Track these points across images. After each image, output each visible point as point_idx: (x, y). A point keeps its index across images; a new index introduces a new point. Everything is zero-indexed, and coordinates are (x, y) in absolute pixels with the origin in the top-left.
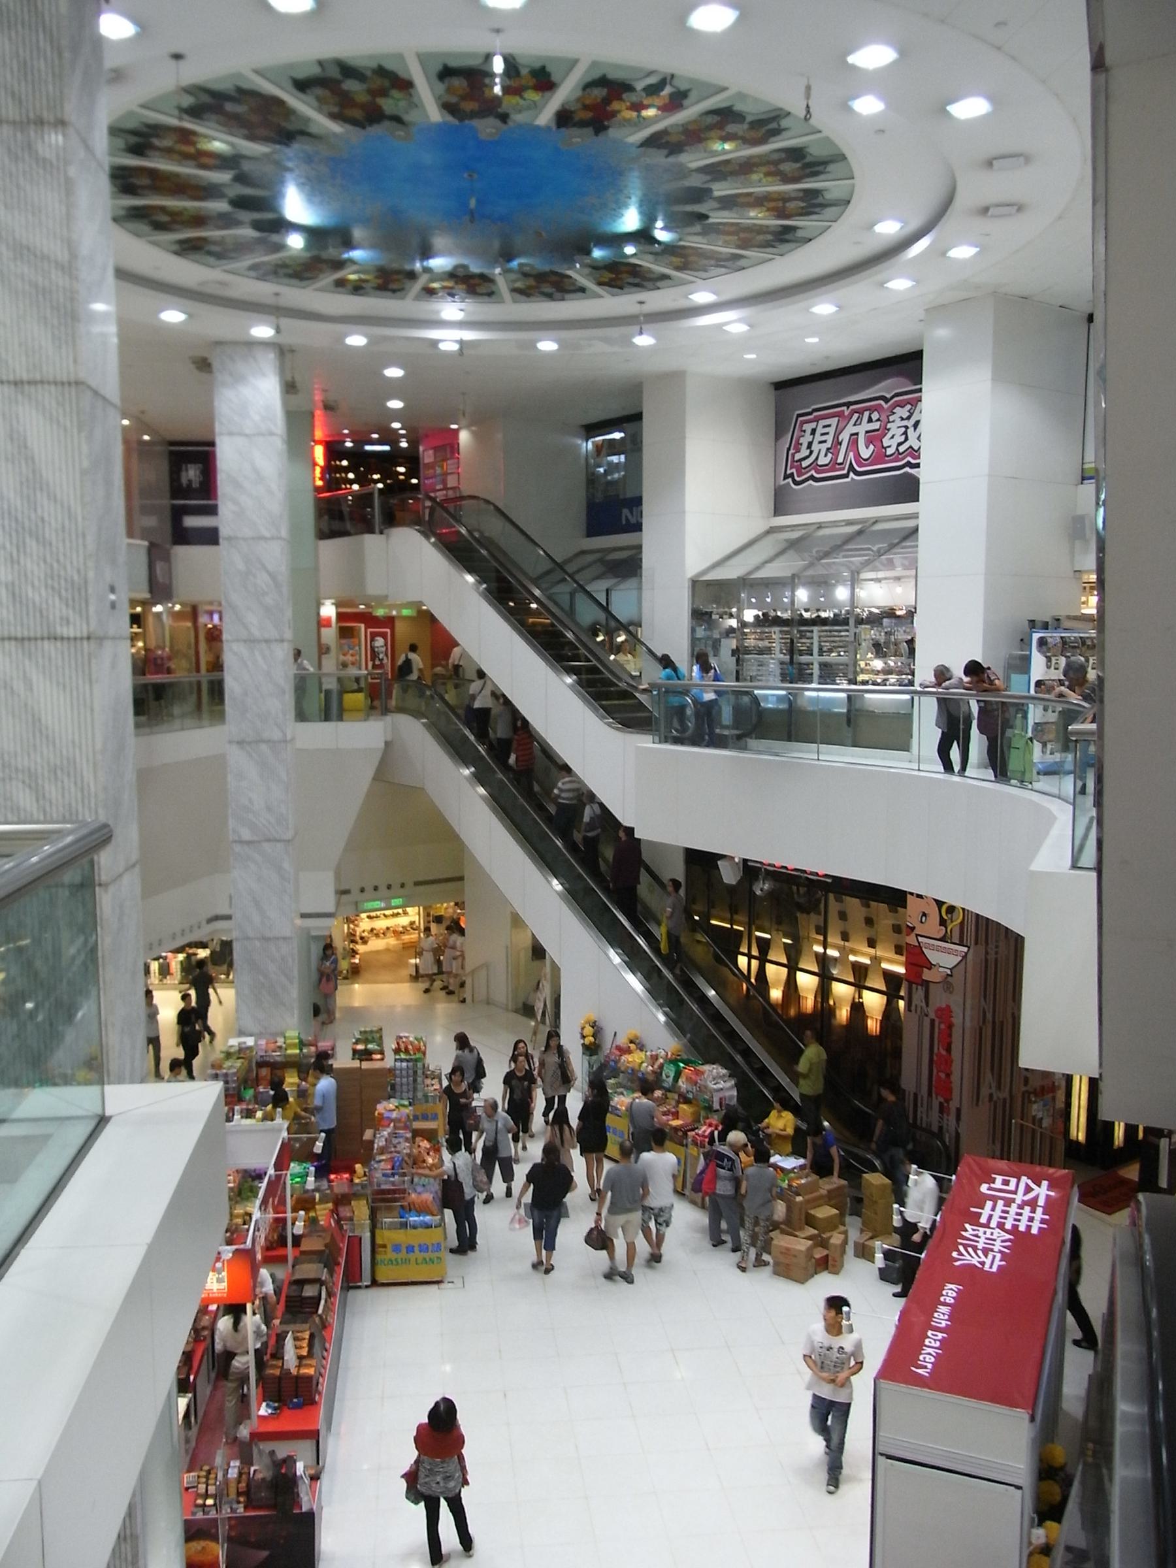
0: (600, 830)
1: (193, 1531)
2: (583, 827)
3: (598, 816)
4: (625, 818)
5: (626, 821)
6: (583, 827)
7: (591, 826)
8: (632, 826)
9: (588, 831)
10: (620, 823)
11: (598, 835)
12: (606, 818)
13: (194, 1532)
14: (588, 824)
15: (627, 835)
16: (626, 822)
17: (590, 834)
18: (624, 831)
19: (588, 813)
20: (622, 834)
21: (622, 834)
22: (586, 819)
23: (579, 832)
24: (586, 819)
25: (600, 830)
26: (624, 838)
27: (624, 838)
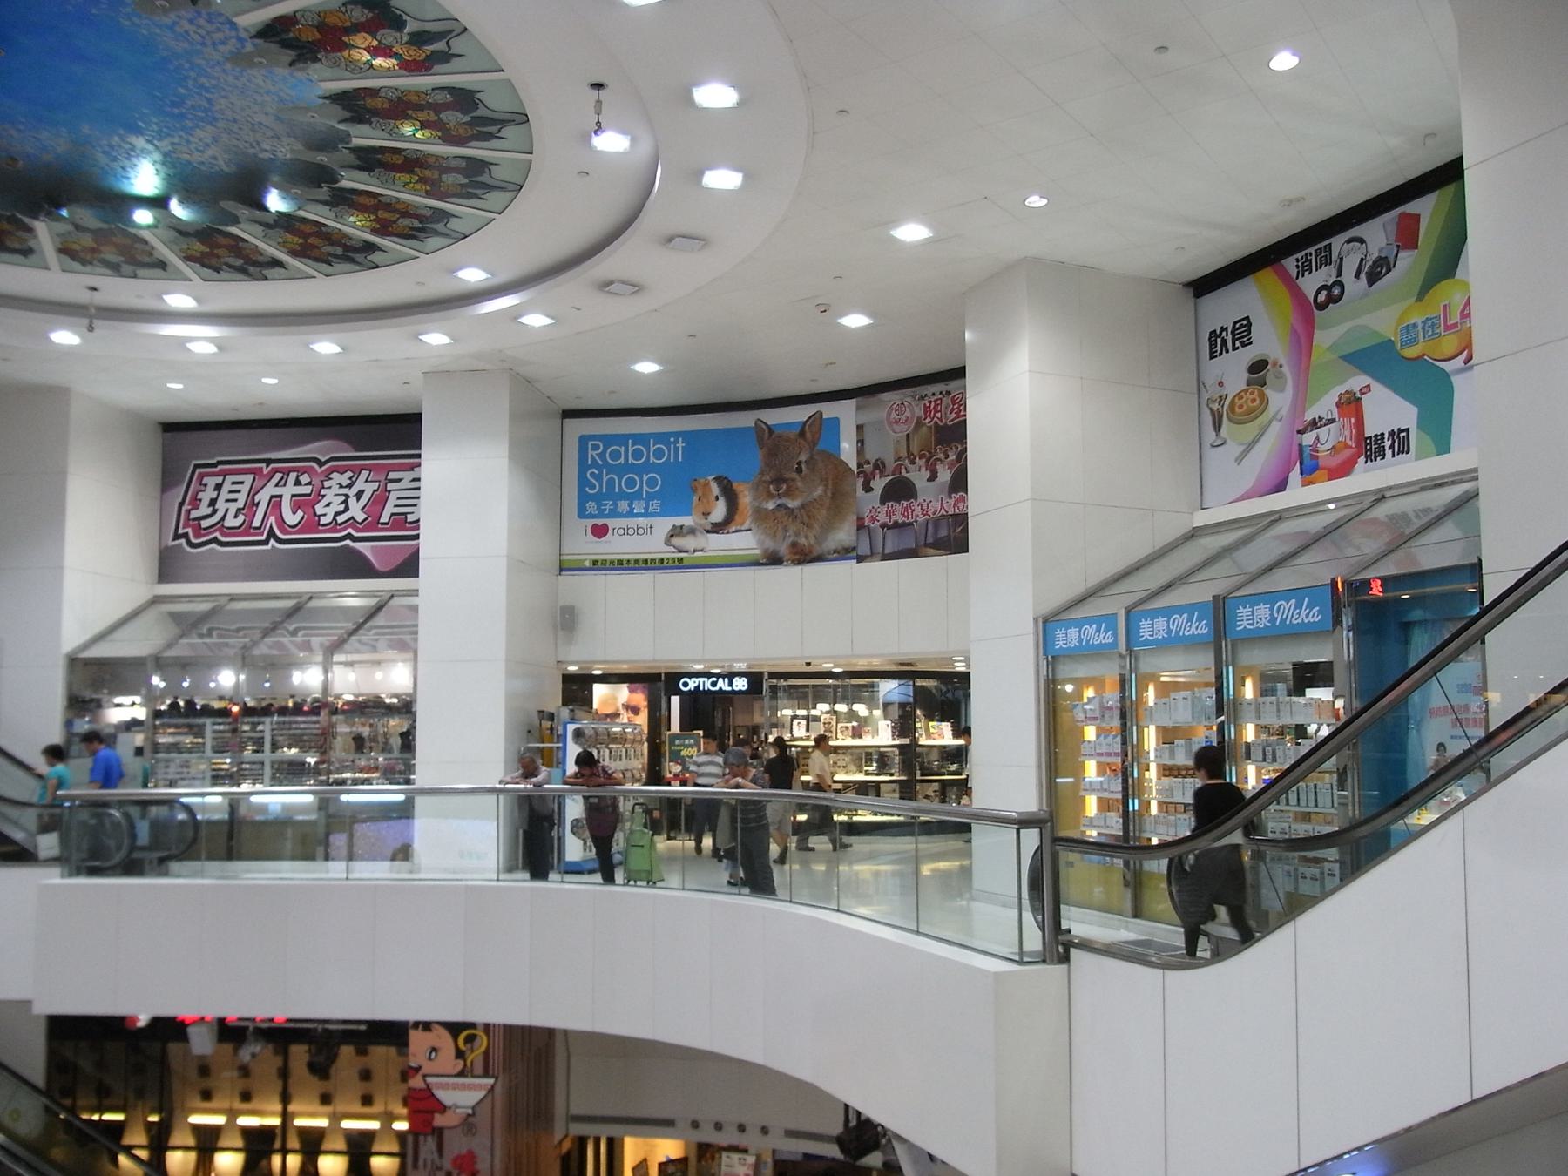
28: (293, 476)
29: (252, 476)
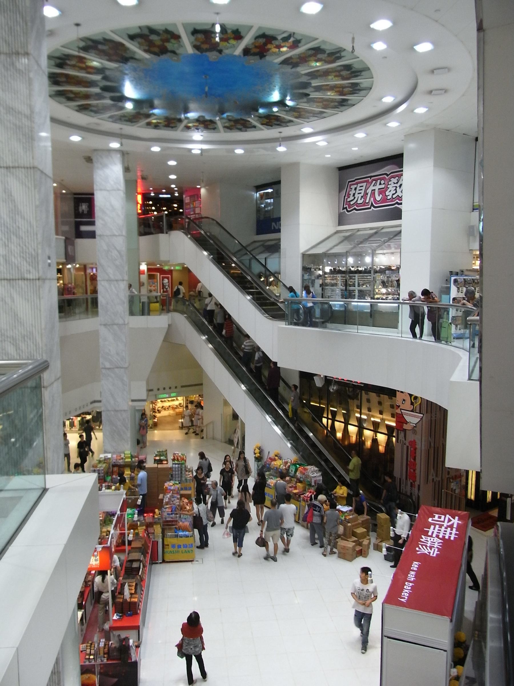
0: (262, 363)
1: (84, 670)
2: (255, 362)
3: (261, 357)
4: (273, 358)
5: (274, 359)
6: (255, 362)
7: (258, 361)
8: (276, 361)
9: (257, 364)
10: (271, 360)
11: (261, 365)
12: (265, 358)
13: (85, 670)
14: (257, 360)
15: (274, 365)
16: (274, 360)
17: (258, 365)
18: (273, 364)
19: (257, 356)
20: (272, 365)
21: (272, 365)
22: (256, 358)
23: (253, 364)
24: (256, 358)
25: (262, 363)
26: (273, 367)
27: (273, 367)
28: (379, 181)
29: (366, 183)
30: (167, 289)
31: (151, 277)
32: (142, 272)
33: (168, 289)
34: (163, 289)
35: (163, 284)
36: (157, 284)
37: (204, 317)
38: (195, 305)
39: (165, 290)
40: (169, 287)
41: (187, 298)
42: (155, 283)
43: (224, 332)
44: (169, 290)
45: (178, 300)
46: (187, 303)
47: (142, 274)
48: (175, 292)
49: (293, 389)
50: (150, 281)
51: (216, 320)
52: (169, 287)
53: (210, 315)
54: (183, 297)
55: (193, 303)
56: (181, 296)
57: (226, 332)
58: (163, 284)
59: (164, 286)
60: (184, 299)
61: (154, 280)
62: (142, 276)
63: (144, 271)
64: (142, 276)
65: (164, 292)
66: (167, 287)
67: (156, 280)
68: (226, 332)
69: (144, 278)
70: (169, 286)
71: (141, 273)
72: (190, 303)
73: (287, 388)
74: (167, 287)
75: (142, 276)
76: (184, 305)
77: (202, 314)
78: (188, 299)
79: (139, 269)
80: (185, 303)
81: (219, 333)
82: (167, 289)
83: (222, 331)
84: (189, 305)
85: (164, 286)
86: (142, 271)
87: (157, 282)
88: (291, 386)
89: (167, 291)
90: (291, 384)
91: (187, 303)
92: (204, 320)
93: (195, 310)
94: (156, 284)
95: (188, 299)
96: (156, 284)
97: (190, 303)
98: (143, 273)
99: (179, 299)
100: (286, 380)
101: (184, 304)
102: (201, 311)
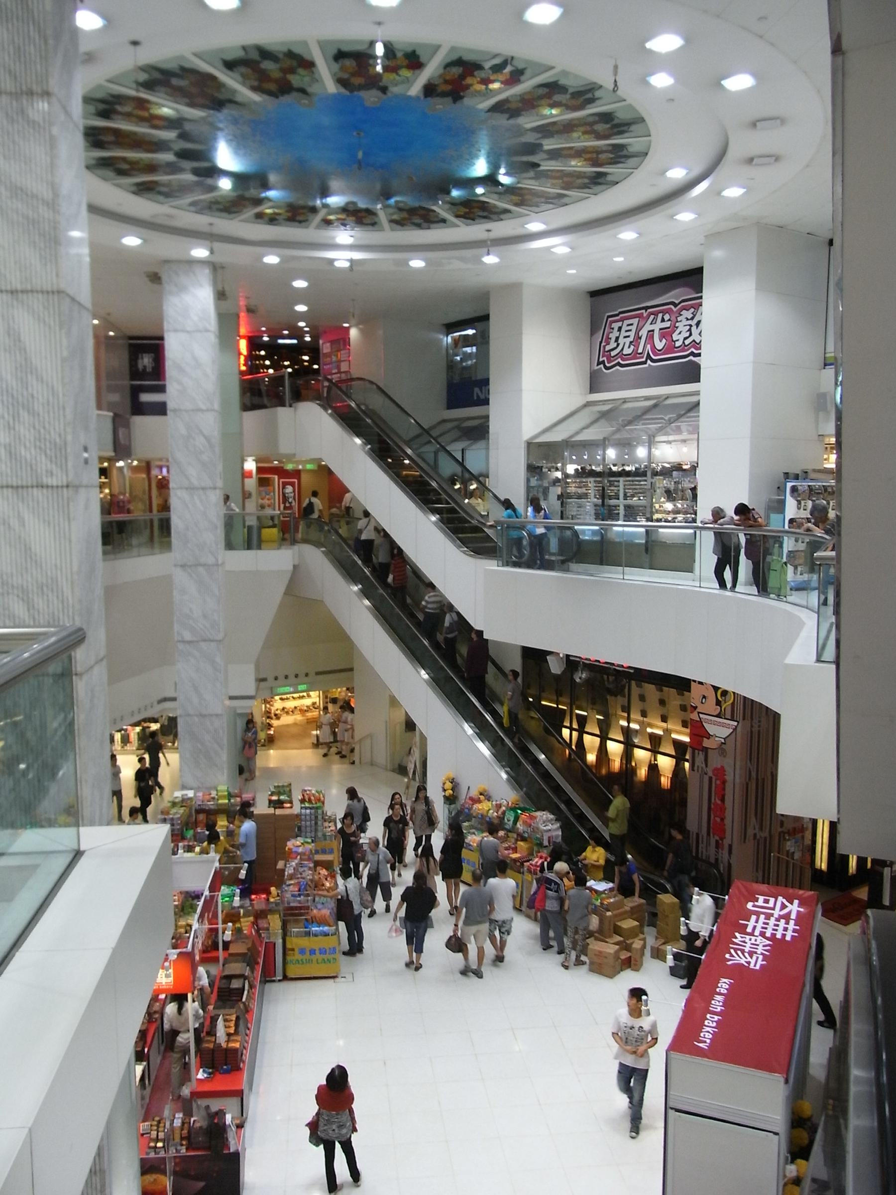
0: (457, 632)
2: (444, 631)
3: (455, 622)
4: (476, 623)
5: (477, 625)
6: (444, 631)
7: (450, 629)
9: (448, 634)
10: (472, 627)
11: (456, 637)
12: (462, 623)
14: (448, 628)
15: (477, 636)
16: (477, 627)
17: (449, 636)
18: (475, 633)
19: (448, 620)
20: (474, 636)
21: (474, 636)
22: (447, 624)
23: (441, 634)
24: (447, 624)
25: (457, 632)
26: (475, 639)
27: (475, 639)
30: (290, 503)
31: (263, 482)
32: (247, 475)
33: (293, 504)
34: (284, 503)
35: (284, 494)
36: (274, 494)
37: (356, 552)
38: (340, 531)
39: (287, 505)
40: (294, 499)
41: (326, 519)
42: (270, 493)
43: (390, 578)
44: (295, 504)
45: (311, 523)
46: (326, 528)
47: (247, 477)
48: (305, 509)
49: (511, 677)
50: (262, 489)
51: (377, 558)
52: (294, 499)
53: (365, 548)
54: (319, 517)
55: (337, 527)
56: (315, 515)
57: (394, 578)
58: (284, 494)
59: (285, 499)
60: (322, 521)
61: (268, 488)
62: (247, 481)
63: (250, 472)
64: (247, 481)
65: (285, 508)
66: (290, 500)
67: (271, 488)
68: (394, 578)
69: (251, 484)
70: (294, 499)
71: (246, 475)
72: (332, 527)
73: (500, 675)
74: (290, 500)
75: (247, 481)
76: (320, 531)
77: (353, 547)
78: (327, 521)
79: (243, 468)
80: (323, 528)
81: (382, 579)
82: (290, 503)
83: (388, 577)
84: (329, 531)
85: (285, 499)
86: (247, 472)
87: (274, 492)
88: (507, 672)
89: (290, 508)
90: (507, 668)
91: (326, 528)
92: (356, 558)
93: (341, 541)
94: (272, 494)
95: (327, 521)
96: (272, 494)
97: (332, 527)
98: (249, 475)
99: (313, 521)
100: (498, 662)
101: (321, 529)
102: (351, 542)
